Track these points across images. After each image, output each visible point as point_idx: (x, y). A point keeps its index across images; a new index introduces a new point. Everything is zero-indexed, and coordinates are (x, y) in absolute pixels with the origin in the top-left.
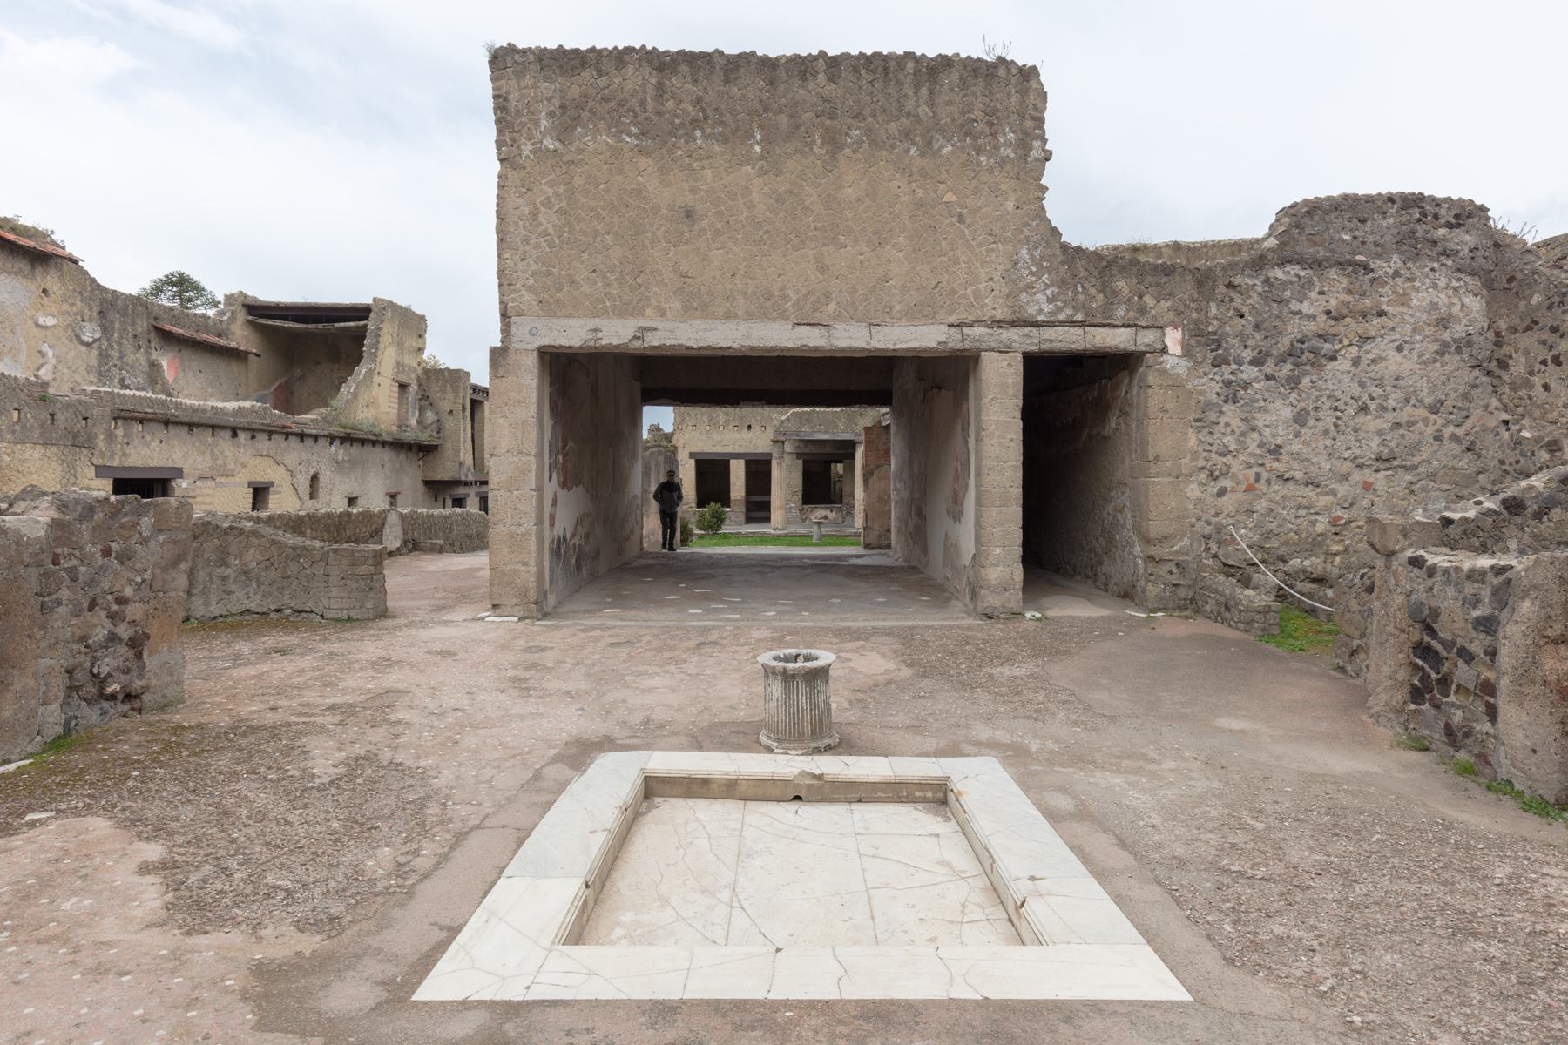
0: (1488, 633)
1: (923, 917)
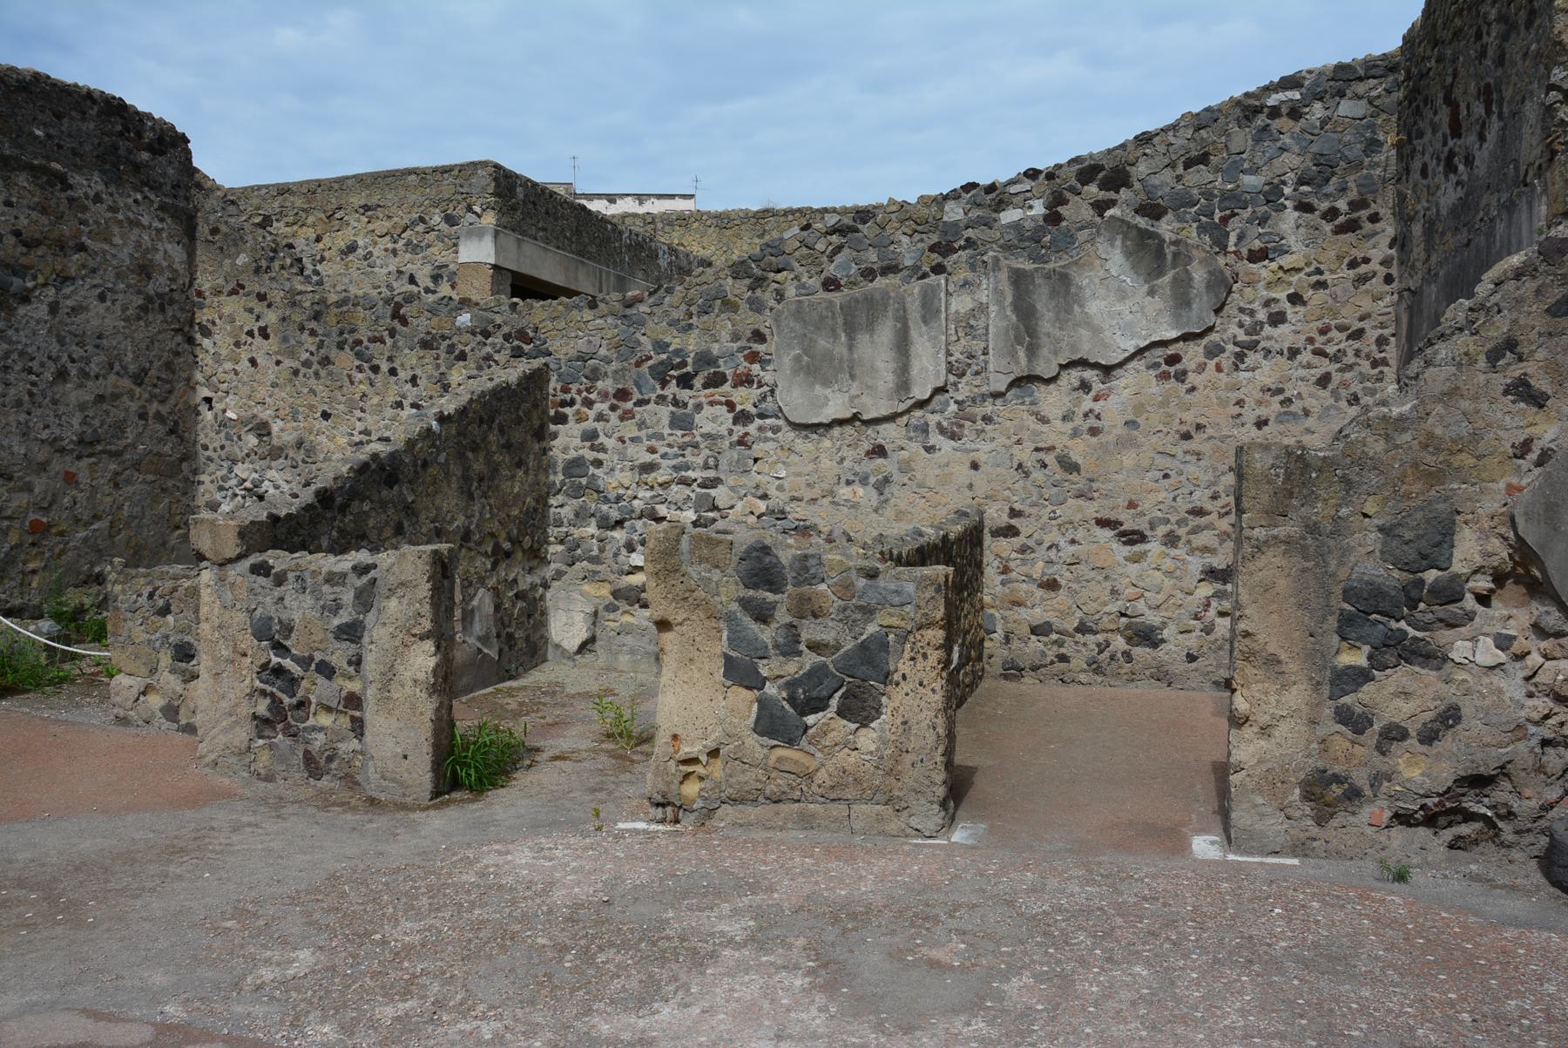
0: (352, 641)
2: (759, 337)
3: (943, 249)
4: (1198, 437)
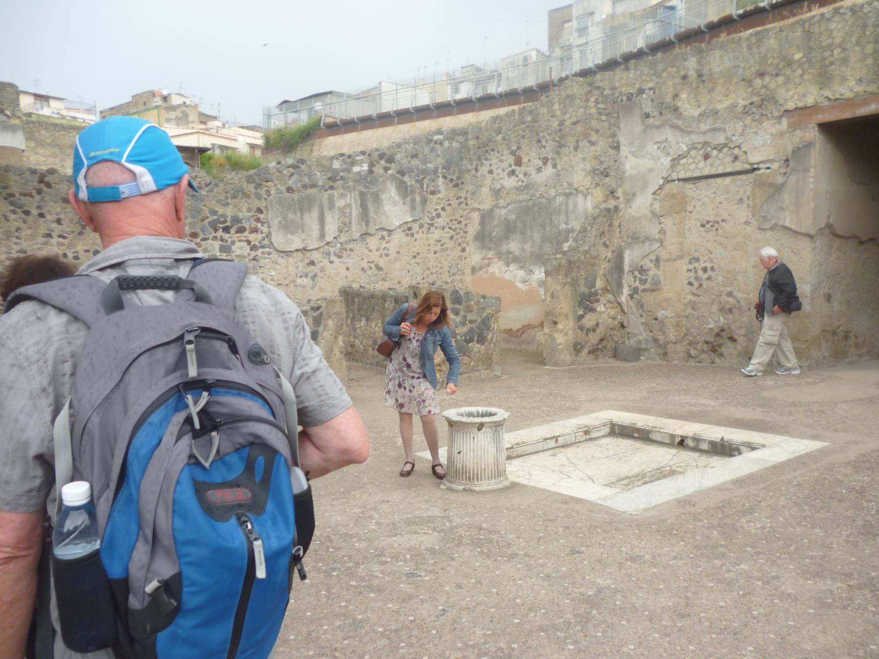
2: (260, 211)
3: (333, 179)
4: (418, 257)
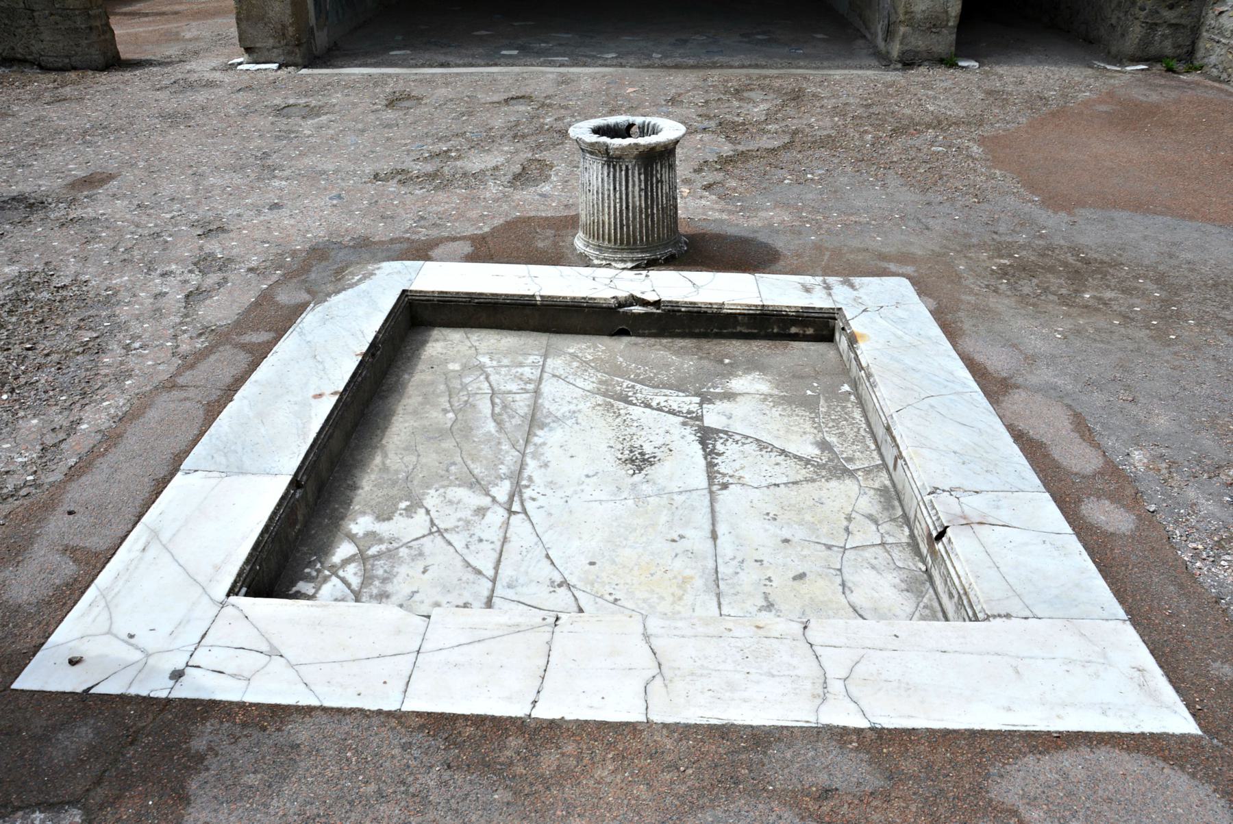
1: (788, 536)
